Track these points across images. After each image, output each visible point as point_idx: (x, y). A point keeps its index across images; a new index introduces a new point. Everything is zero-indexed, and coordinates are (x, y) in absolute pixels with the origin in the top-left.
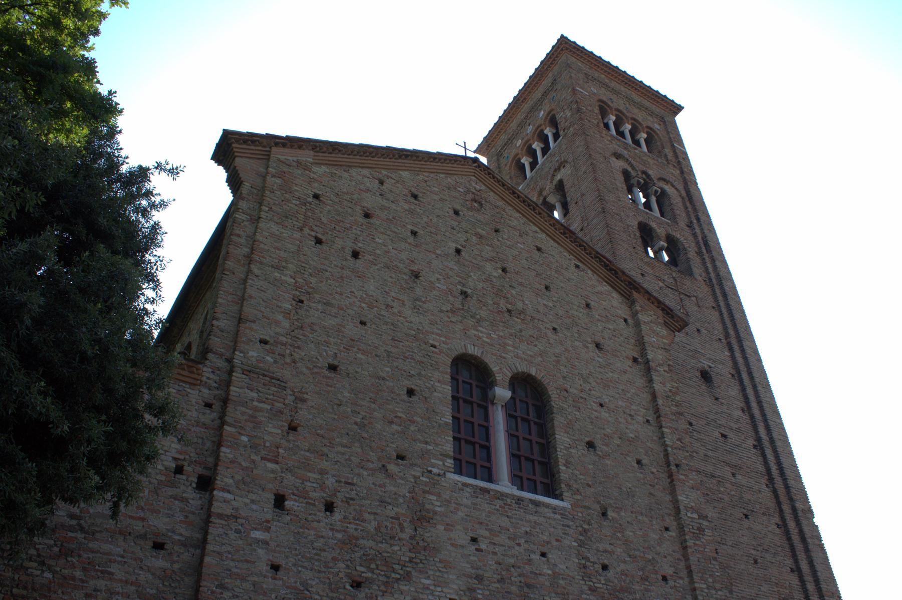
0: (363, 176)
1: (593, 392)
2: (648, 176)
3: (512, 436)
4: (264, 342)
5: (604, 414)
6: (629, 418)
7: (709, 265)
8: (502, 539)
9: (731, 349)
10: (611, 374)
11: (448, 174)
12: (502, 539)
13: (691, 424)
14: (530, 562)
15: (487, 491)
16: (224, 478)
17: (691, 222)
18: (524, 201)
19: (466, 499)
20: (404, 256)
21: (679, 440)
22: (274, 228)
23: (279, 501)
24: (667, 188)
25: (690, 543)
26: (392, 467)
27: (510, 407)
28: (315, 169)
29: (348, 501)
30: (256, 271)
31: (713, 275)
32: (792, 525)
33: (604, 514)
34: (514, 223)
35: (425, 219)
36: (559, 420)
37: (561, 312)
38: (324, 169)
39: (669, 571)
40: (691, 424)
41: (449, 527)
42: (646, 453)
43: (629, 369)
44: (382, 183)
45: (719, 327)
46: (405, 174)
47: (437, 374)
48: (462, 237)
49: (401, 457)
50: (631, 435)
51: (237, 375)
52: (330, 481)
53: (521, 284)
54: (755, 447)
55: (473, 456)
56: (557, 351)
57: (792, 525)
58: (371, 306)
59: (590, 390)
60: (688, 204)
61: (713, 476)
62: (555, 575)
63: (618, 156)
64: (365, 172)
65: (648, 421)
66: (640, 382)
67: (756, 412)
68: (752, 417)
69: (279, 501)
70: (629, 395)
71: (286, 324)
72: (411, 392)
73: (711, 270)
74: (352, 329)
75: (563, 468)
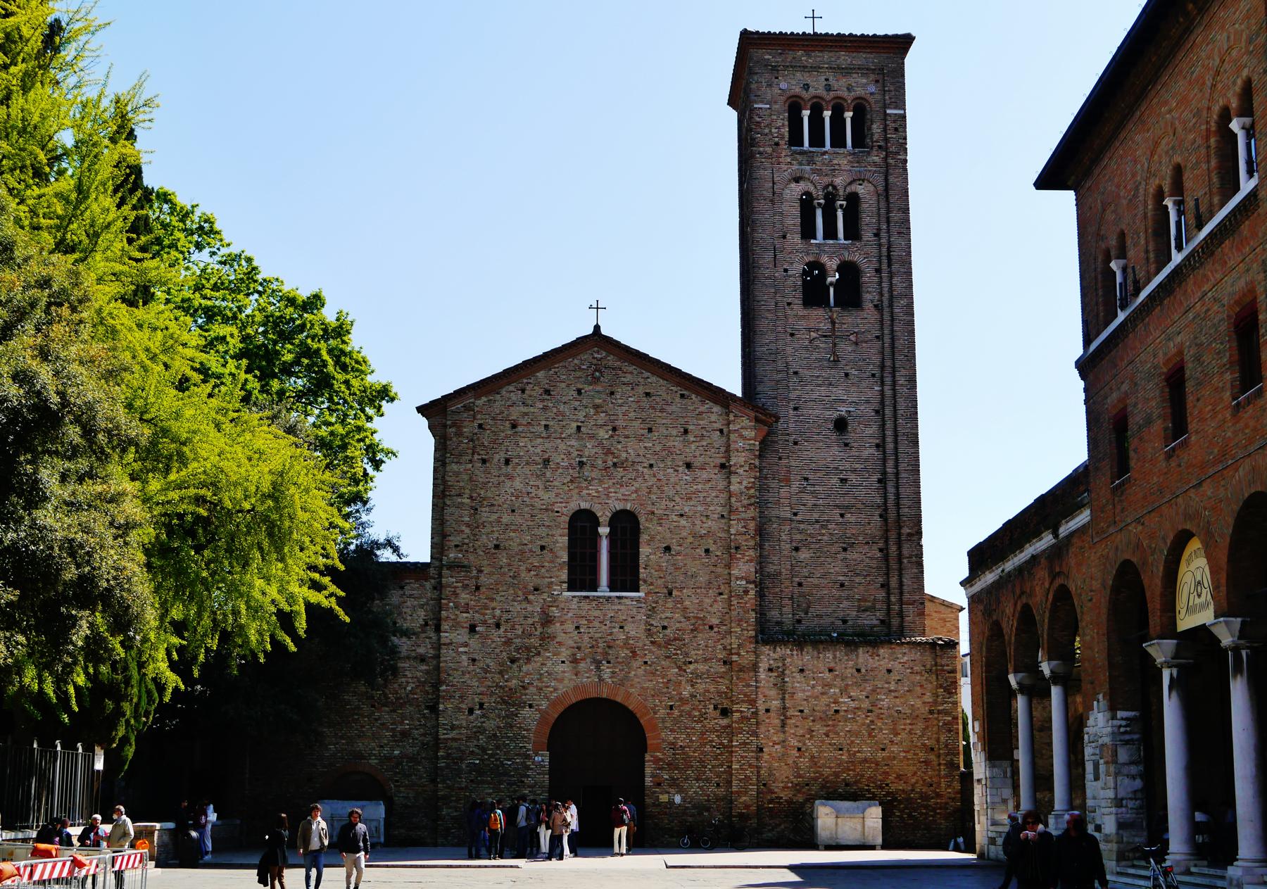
0: (511, 392)
2: (835, 187)
4: (456, 546)
5: (683, 522)
6: (704, 519)
8: (596, 624)
9: (882, 384)
11: (574, 356)
12: (596, 624)
13: (806, 479)
14: (611, 634)
15: (587, 597)
16: (445, 626)
17: (879, 229)
19: (574, 605)
20: (538, 450)
22: (455, 467)
23: (472, 629)
24: (861, 189)
25: (735, 602)
26: (531, 597)
27: (611, 536)
28: (478, 402)
29: (507, 621)
30: (448, 502)
32: (893, 548)
33: (670, 594)
34: (629, 378)
35: (555, 410)
36: (644, 538)
38: (484, 399)
39: (715, 621)
40: (806, 479)
41: (562, 623)
42: (715, 543)
44: (523, 391)
45: (876, 359)
46: (541, 374)
47: (560, 531)
48: (581, 415)
49: (536, 589)
51: (445, 572)
52: (498, 612)
53: (627, 437)
54: (880, 481)
55: (581, 577)
57: (893, 548)
58: (517, 497)
60: (883, 204)
61: (817, 521)
62: (628, 638)
64: (511, 388)
66: (722, 485)
67: (890, 446)
68: (884, 452)
69: (472, 629)
71: (467, 531)
72: (543, 548)
73: (886, 290)
75: (642, 570)
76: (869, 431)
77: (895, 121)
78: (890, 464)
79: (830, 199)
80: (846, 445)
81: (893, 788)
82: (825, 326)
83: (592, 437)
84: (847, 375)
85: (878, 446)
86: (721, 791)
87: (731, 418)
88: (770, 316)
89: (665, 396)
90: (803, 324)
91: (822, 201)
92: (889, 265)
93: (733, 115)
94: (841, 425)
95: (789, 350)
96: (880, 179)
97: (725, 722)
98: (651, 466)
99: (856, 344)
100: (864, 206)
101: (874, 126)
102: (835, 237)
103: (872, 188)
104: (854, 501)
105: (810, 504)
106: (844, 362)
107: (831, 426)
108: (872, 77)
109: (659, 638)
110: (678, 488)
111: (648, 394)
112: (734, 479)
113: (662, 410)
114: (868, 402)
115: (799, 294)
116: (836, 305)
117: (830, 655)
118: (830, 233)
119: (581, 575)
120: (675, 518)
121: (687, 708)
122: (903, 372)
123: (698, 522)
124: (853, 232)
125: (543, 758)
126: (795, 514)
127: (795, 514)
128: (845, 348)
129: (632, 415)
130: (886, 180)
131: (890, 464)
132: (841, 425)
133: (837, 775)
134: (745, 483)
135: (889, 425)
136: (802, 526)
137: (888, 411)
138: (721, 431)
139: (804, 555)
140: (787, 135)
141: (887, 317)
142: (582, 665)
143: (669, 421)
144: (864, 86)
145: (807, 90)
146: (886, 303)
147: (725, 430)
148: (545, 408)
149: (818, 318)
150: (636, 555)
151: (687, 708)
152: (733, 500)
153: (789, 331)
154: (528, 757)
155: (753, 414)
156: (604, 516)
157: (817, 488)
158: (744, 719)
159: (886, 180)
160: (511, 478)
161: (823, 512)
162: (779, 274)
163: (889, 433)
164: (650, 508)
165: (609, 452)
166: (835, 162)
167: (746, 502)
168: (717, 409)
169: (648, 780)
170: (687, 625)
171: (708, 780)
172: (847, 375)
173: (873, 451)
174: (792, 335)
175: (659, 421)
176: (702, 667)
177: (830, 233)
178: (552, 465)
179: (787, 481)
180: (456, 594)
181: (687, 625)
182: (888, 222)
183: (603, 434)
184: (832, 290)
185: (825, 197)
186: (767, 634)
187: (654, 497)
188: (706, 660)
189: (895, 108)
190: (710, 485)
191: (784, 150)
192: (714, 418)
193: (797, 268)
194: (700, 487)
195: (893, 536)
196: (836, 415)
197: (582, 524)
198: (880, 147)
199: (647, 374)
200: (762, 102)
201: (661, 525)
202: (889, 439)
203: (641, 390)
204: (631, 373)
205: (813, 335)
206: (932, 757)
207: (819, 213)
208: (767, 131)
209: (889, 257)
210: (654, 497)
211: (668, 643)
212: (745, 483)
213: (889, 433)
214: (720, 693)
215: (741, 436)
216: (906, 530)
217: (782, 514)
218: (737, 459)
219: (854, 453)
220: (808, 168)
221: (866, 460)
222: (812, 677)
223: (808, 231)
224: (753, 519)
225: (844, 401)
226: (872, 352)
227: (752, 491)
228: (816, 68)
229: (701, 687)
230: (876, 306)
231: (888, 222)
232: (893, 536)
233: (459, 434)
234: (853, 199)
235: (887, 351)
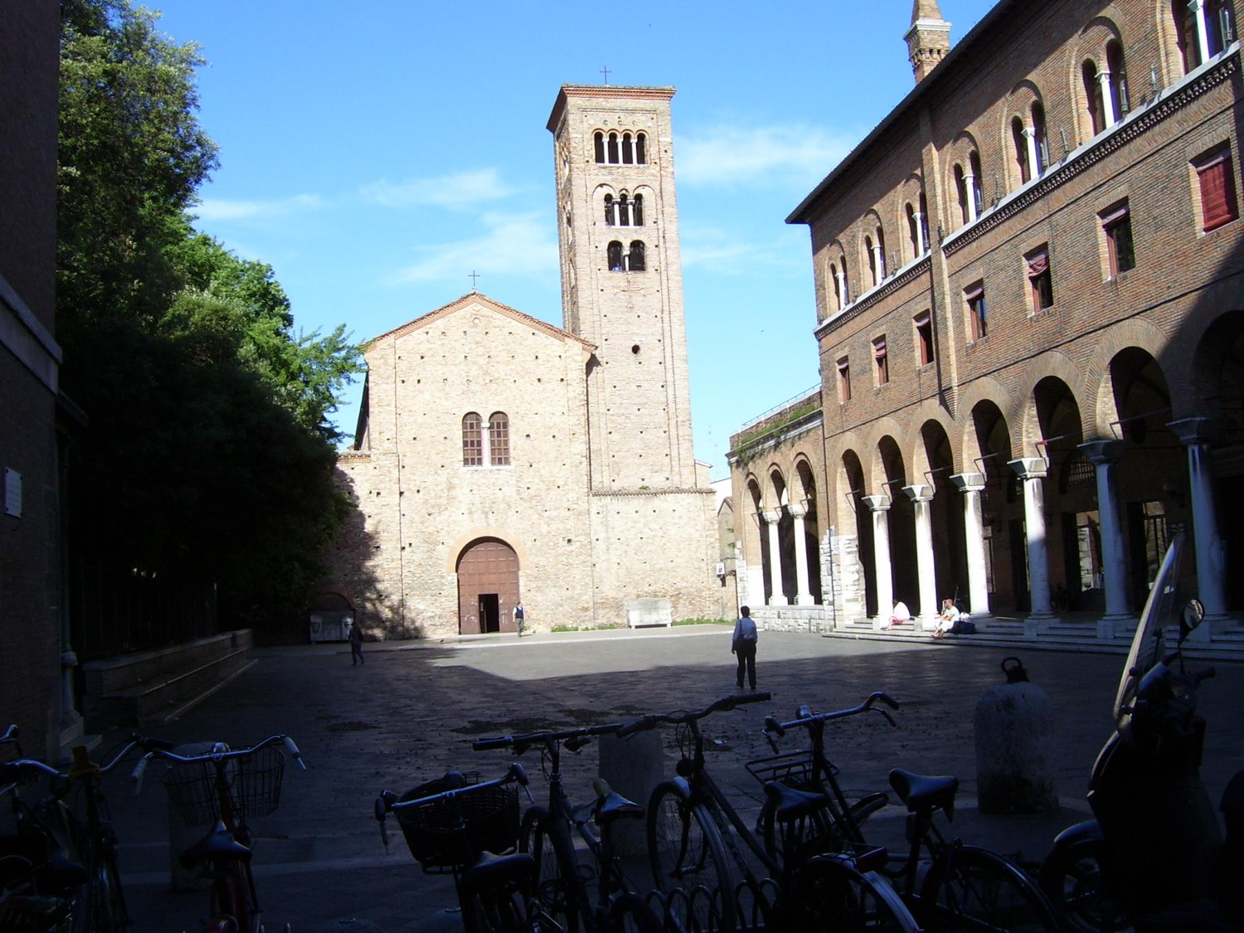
0: (417, 335)
3: (492, 443)
7: (663, 256)
19: (469, 476)
22: (384, 386)
34: (498, 323)
37: (519, 369)
39: (560, 483)
52: (418, 483)
60: (659, 202)
63: (601, 185)
67: (669, 364)
74: (421, 419)
76: (654, 354)
78: (670, 375)
79: (624, 197)
81: (679, 585)
82: (623, 284)
83: (475, 363)
86: (569, 593)
94: (636, 349)
95: (601, 301)
96: (656, 185)
97: (569, 548)
108: (650, 116)
109: (525, 495)
117: (636, 502)
119: (472, 455)
121: (546, 540)
124: (639, 221)
125: (453, 577)
128: (637, 299)
129: (501, 348)
131: (670, 375)
133: (643, 579)
135: (668, 349)
137: (667, 340)
139: (615, 436)
141: (664, 278)
142: (475, 516)
148: (443, 345)
149: (618, 276)
150: (506, 442)
151: (546, 540)
154: (443, 577)
156: (485, 417)
158: (583, 546)
160: (421, 392)
162: (593, 249)
163: (668, 354)
165: (487, 373)
168: (557, 342)
169: (522, 589)
170: (542, 486)
171: (560, 587)
176: (553, 514)
177: (624, 222)
178: (449, 382)
180: (389, 472)
181: (542, 486)
183: (483, 361)
186: (595, 492)
188: (556, 509)
192: (555, 348)
193: (604, 246)
195: (673, 422)
197: (471, 420)
203: (506, 331)
204: (499, 318)
206: (703, 565)
207: (616, 207)
211: (532, 498)
213: (668, 354)
214: (567, 530)
216: (680, 419)
219: (645, 368)
221: (654, 373)
222: (625, 516)
223: (610, 219)
226: (655, 302)
228: (612, 110)
229: (554, 527)
232: (673, 422)
233: (386, 363)
234: (639, 198)
235: (666, 300)
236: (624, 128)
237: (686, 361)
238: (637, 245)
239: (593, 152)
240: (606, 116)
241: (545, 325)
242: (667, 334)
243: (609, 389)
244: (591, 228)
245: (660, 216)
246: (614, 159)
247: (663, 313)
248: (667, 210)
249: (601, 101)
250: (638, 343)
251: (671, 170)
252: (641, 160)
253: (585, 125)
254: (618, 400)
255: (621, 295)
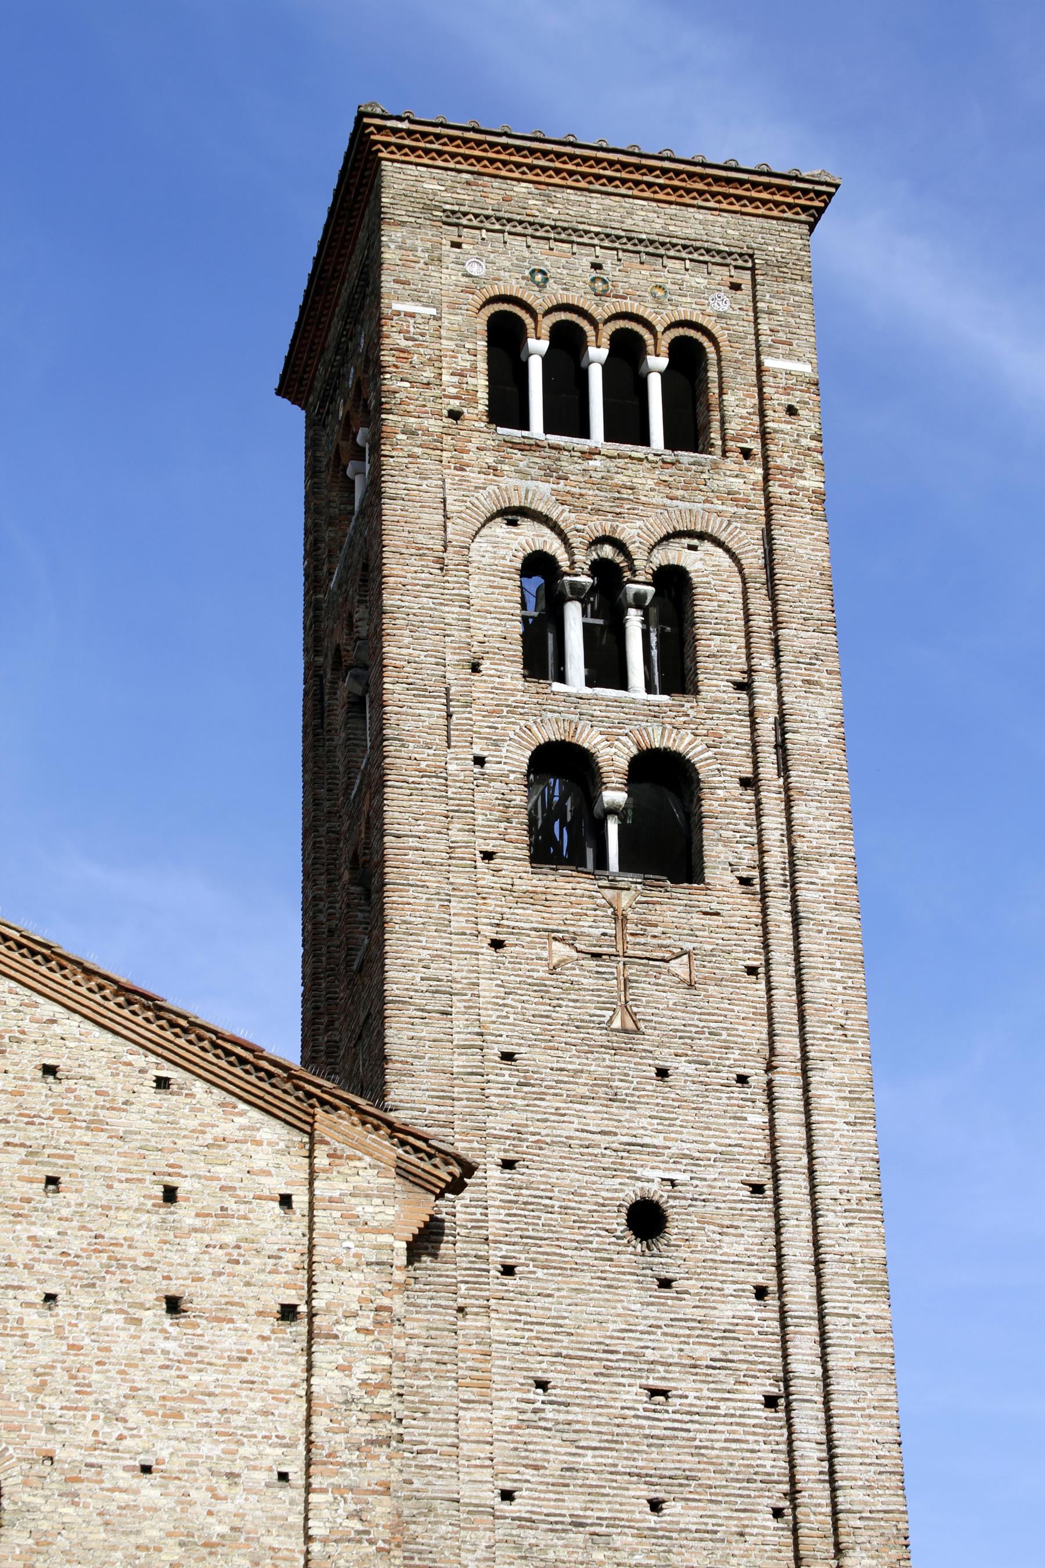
1: (128, 1442)
2: (620, 546)
5: (148, 1490)
7: (774, 823)
10: (194, 1378)
13: (542, 1385)
17: (750, 671)
18: (20, 946)
21: (357, 1515)
31: (776, 858)
37: (76, 1244)
40: (542, 1385)
43: (256, 1345)
50: (224, 1529)
54: (770, 1402)
56: (44, 1359)
59: (121, 1438)
60: (760, 603)
65: (283, 1477)
67: (801, 1297)
70: (237, 1420)
73: (774, 836)
76: (732, 1247)
77: (787, 390)
79: (608, 577)
80: (665, 1283)
82: (595, 928)
84: (662, 1073)
85: (761, 1293)
87: (321, 1161)
88: (433, 881)
89: (103, 1079)
90: (529, 917)
91: (585, 580)
92: (784, 769)
93: (293, 419)
94: (646, 1220)
95: (488, 989)
98: (50, 1298)
99: (691, 986)
100: (703, 607)
101: (729, 398)
102: (622, 683)
103: (726, 560)
104: (690, 1462)
105: (554, 1467)
106: (652, 1036)
107: (619, 1222)
108: (722, 274)
110: (137, 1376)
111: (49, 1070)
112: (325, 1355)
113: (95, 1125)
114: (725, 1157)
115: (518, 831)
116: (625, 866)
118: (606, 668)
120: (126, 1479)
122: (833, 1073)
123: (199, 1495)
124: (676, 673)
126: (507, 1496)
127: (507, 1496)
128: (658, 998)
130: (768, 538)
132: (646, 1220)
134: (360, 1370)
136: (530, 1536)
137: (794, 1188)
138: (286, 1201)
140: (483, 395)
143: (119, 1162)
144: (698, 293)
145: (542, 285)
146: (776, 876)
147: (300, 1201)
152: (320, 1423)
153: (490, 932)
155: (391, 1152)
157: (576, 1414)
159: (768, 538)
161: (594, 1493)
162: (459, 767)
164: (40, 1440)
166: (620, 479)
167: (362, 1432)
172: (662, 1073)
173: (748, 1305)
174: (497, 945)
175: (84, 1157)
177: (606, 668)
179: (485, 1384)
182: (777, 654)
184: (613, 828)
185: (600, 567)
187: (54, 1403)
189: (789, 356)
190: (242, 1373)
191: (480, 435)
194: (209, 1378)
196: (631, 1194)
198: (746, 453)
199: (49, 1009)
200: (417, 300)
201: (73, 1498)
202: (799, 1273)
203: (26, 1060)
205: (561, 950)
207: (574, 616)
208: (428, 374)
209: (781, 747)
210: (54, 1403)
212: (360, 1370)
215: (352, 1219)
217: (467, 1493)
218: (339, 1293)
219: (687, 1308)
220: (545, 488)
223: (541, 658)
224: (387, 1489)
225: (655, 1151)
227: (383, 1397)
228: (565, 233)
230: (745, 881)
231: (777, 654)
234: (674, 583)
236: (612, 306)
237: (883, 1289)
238: (664, 775)
239: (481, 383)
240: (541, 254)
241: (220, 1043)
242: (793, 1159)
243: (510, 1399)
244: (456, 676)
245: (764, 662)
246: (568, 417)
247: (781, 1071)
248: (796, 638)
249: (523, 195)
250: (656, 1191)
251: (812, 481)
252: (688, 431)
253: (449, 277)
254: (554, 1452)
255: (585, 975)
